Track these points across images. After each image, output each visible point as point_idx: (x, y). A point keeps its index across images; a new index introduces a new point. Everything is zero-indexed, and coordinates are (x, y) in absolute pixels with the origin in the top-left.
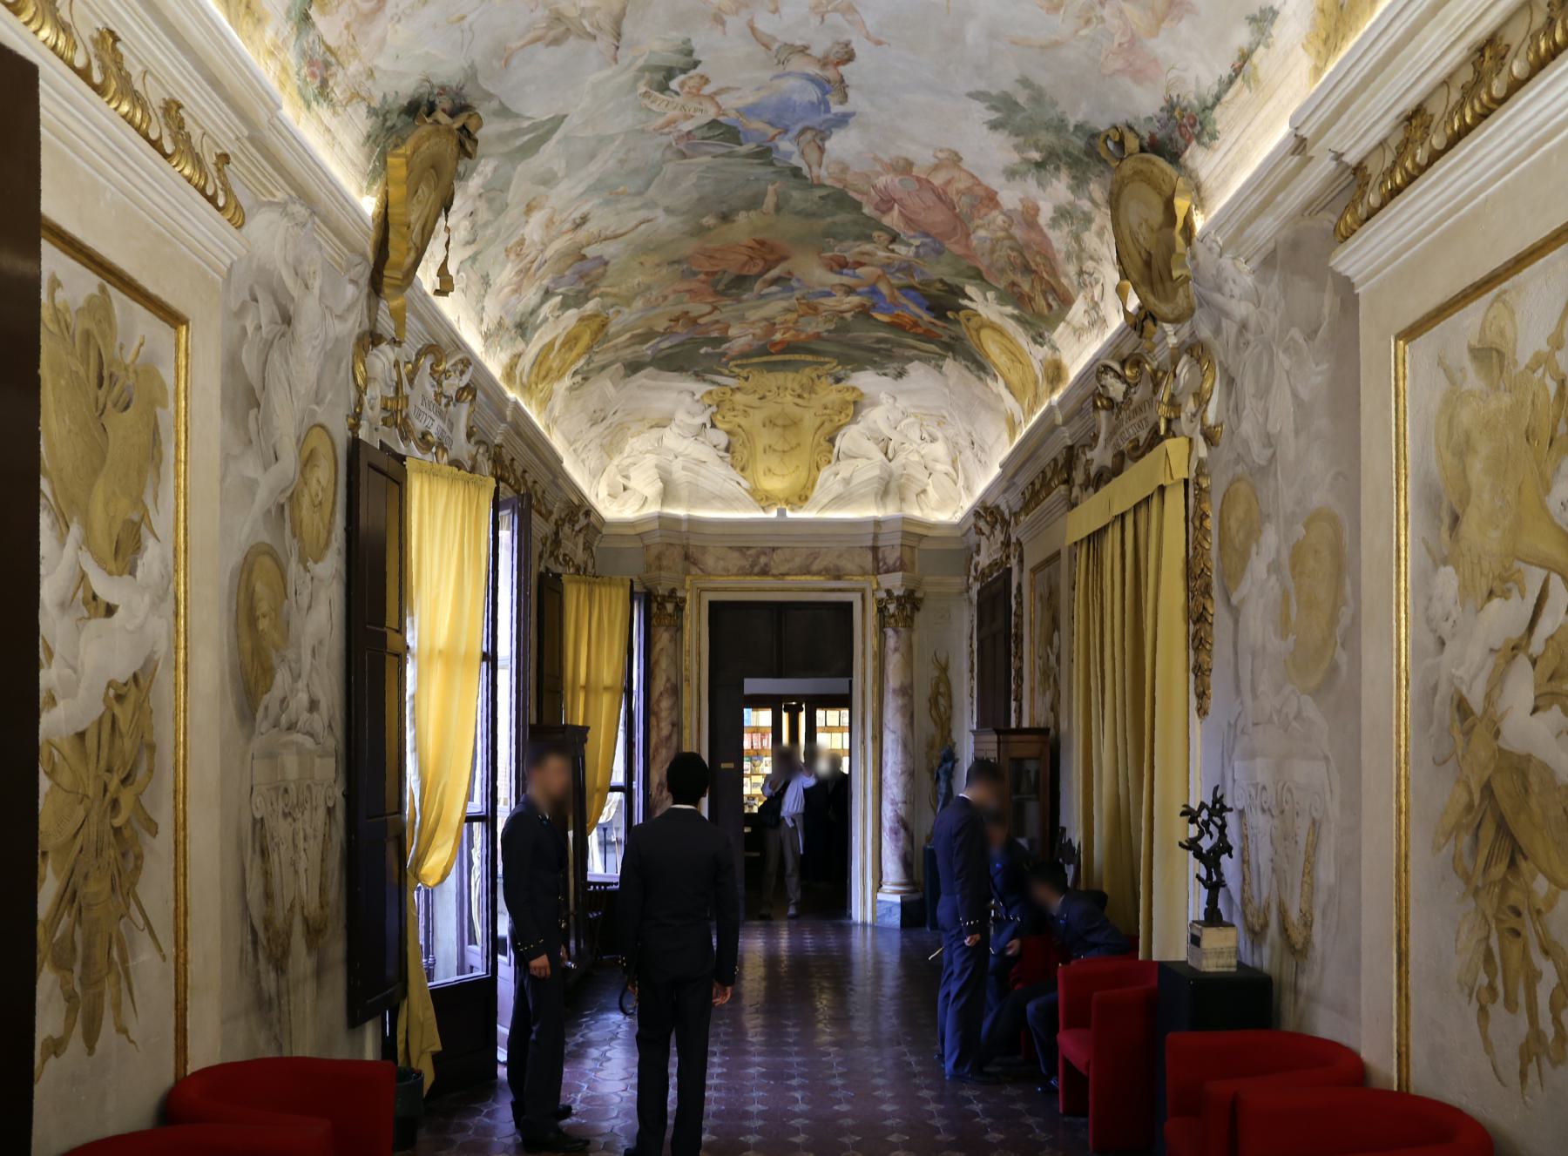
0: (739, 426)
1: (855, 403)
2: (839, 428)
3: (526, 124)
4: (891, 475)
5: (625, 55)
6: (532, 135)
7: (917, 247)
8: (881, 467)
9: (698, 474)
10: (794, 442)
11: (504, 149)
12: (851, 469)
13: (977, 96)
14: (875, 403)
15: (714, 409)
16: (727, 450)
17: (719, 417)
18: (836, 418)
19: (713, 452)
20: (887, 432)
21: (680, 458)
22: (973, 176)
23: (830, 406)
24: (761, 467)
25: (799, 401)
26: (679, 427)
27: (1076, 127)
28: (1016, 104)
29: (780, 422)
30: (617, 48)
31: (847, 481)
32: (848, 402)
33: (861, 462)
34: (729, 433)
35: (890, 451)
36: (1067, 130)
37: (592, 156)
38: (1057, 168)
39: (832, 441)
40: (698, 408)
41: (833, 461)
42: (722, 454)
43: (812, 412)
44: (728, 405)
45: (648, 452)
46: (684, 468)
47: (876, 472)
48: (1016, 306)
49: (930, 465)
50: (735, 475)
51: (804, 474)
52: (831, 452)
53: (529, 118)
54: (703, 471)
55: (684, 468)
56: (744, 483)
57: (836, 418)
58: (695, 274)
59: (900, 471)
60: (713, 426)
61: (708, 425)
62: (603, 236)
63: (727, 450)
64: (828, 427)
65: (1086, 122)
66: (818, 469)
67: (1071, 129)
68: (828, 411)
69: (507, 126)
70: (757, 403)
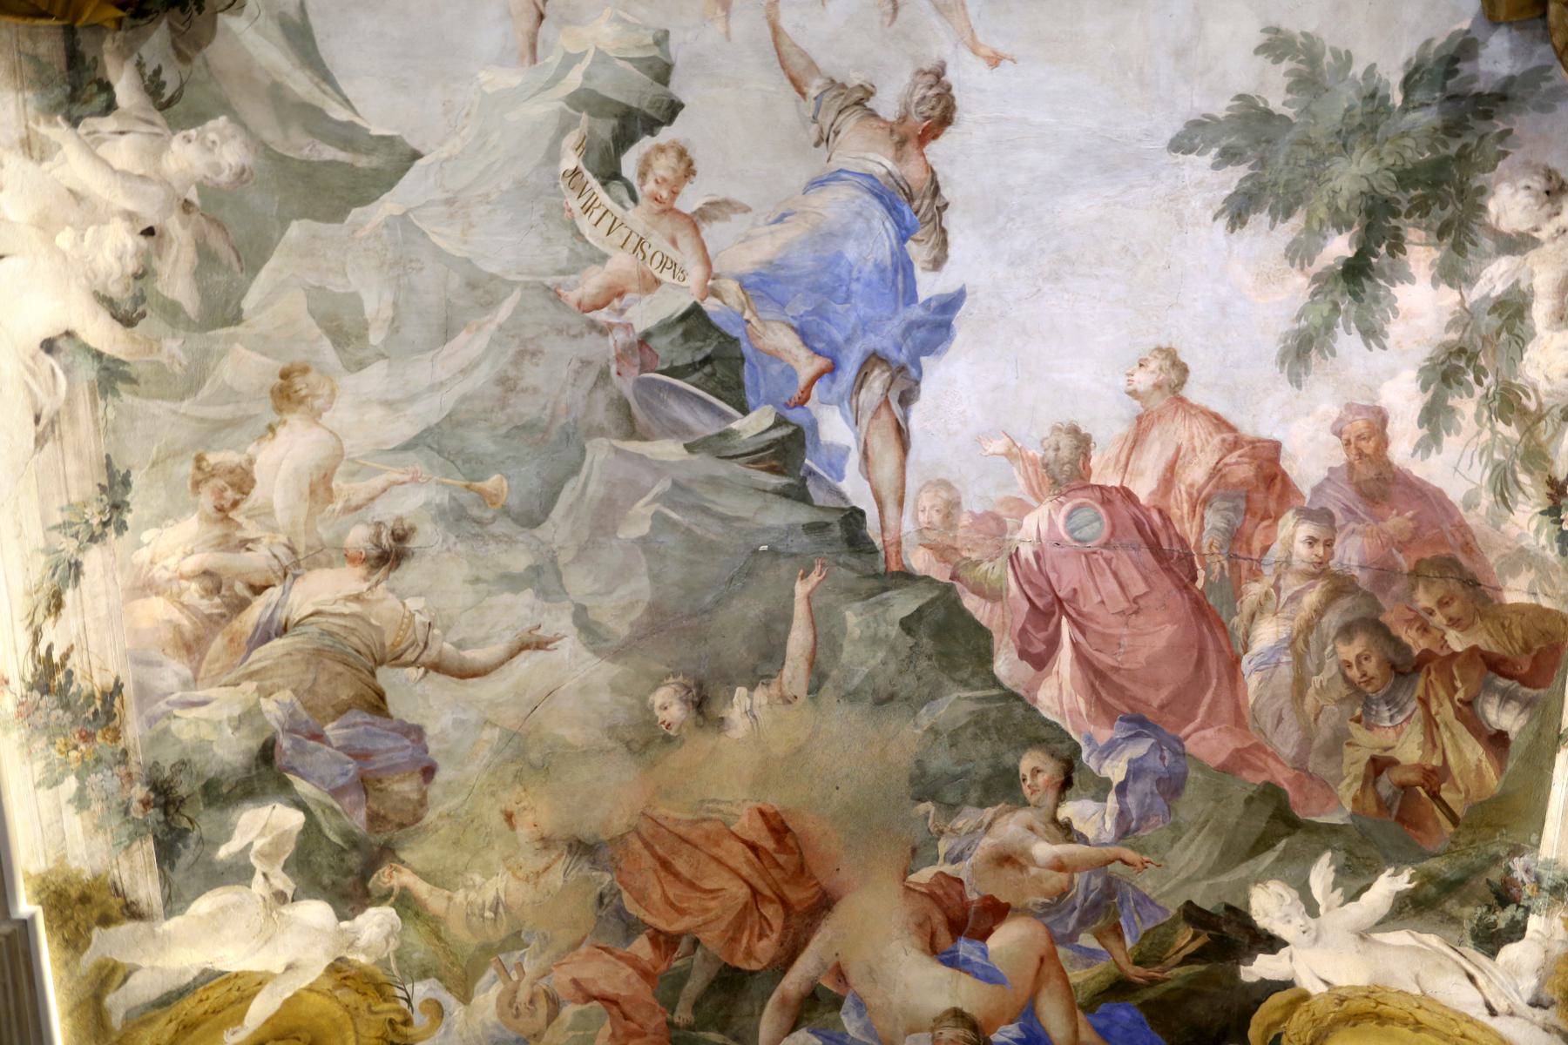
3: (339, 114)
5: (559, 40)
6: (342, 156)
7: (1122, 789)
11: (271, 134)
13: (1182, 144)
22: (1219, 422)
27: (1408, 85)
28: (1268, 115)
30: (541, 17)
36: (1389, 111)
37: (447, 332)
38: (1397, 246)
48: (1396, 858)
53: (346, 102)
58: (631, 927)
62: (431, 655)
65: (1428, 42)
67: (1397, 98)
69: (301, 84)
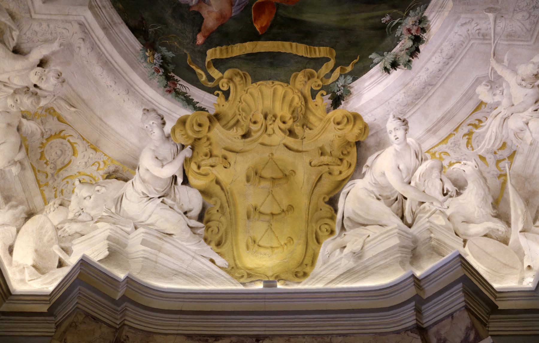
0: (218, 182)
1: (358, 144)
2: (340, 184)
4: (415, 241)
8: (400, 236)
9: (160, 250)
10: (285, 203)
12: (361, 241)
14: (381, 145)
15: (187, 153)
16: (200, 218)
17: (194, 167)
18: (336, 169)
19: (183, 220)
20: (399, 188)
21: (141, 230)
23: (328, 150)
24: (242, 239)
25: (290, 141)
26: (143, 181)
29: (267, 173)
31: (358, 255)
32: (348, 143)
33: (372, 230)
34: (204, 193)
35: (407, 213)
39: (333, 202)
40: (167, 150)
41: (337, 230)
42: (194, 223)
43: (307, 159)
44: (204, 148)
45: (101, 219)
46: (144, 242)
47: (395, 241)
49: (461, 228)
50: (209, 251)
51: (299, 249)
52: (333, 218)
54: (167, 246)
55: (144, 242)
56: (220, 261)
57: (336, 169)
59: (426, 235)
60: (186, 182)
61: (180, 180)
63: (200, 218)
64: (326, 185)
66: (319, 242)
68: (326, 159)
70: (239, 144)
